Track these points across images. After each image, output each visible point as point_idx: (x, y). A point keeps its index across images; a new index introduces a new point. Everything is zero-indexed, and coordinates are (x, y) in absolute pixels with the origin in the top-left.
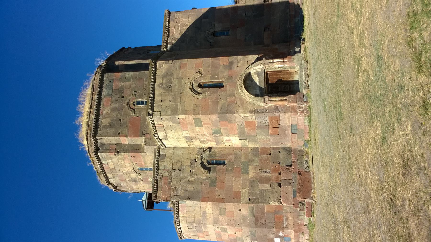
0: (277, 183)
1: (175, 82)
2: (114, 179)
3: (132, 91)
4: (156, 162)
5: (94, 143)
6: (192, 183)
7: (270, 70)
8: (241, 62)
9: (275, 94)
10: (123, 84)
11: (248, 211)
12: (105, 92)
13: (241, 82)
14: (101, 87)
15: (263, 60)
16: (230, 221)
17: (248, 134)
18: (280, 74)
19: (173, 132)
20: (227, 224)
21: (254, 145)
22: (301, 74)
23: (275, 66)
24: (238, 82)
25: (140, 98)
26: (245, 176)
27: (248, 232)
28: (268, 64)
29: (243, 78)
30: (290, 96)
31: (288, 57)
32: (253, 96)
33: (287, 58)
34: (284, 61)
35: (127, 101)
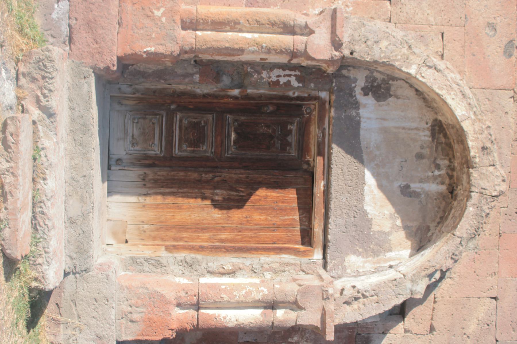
7: (287, 258)
8: (472, 327)
9: (262, 91)
13: (483, 184)
15: (339, 329)
18: (223, 229)
22: (82, 200)
23: (257, 281)
24: (503, 187)
28: (306, 291)
29: (470, 210)
30: (161, 50)
31: (170, 335)
32: (412, 71)
33: (175, 326)
34: (197, 307)
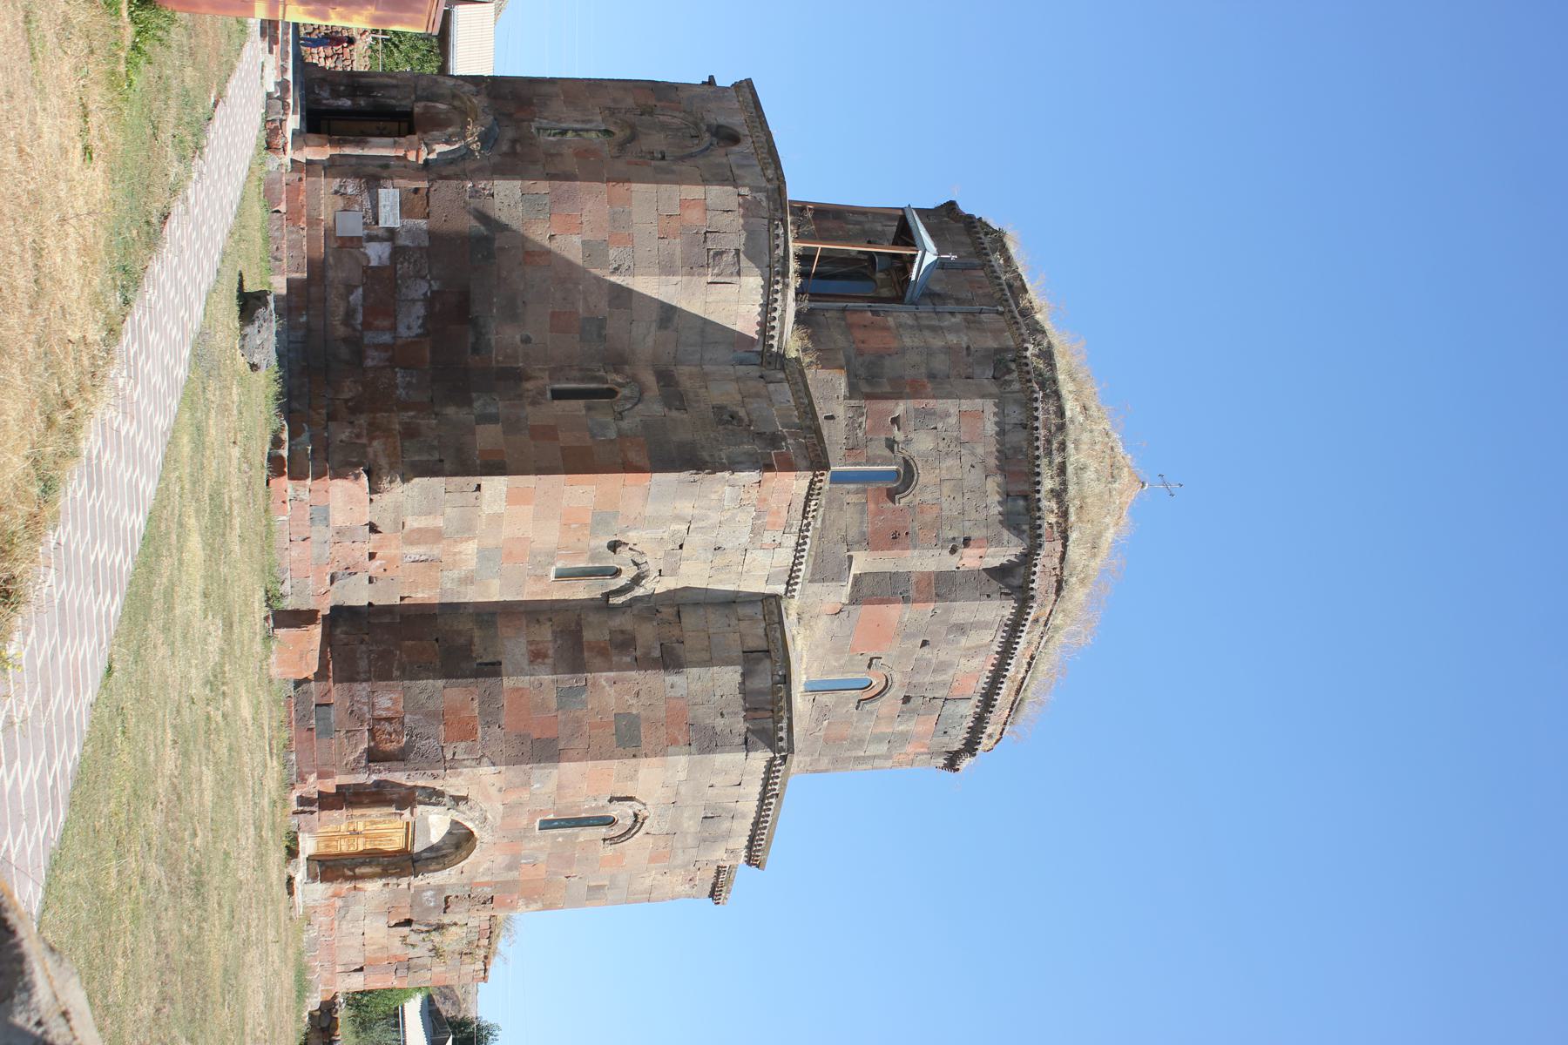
0: (380, 532)
1: (690, 824)
2: (1007, 420)
3: (872, 713)
4: (803, 567)
5: (1033, 581)
6: (678, 518)
8: (481, 870)
10: (901, 728)
11: (493, 339)
12: (968, 709)
14: (980, 722)
16: (564, 299)
17: (472, 693)
19: (718, 694)
20: (581, 287)
21: (455, 628)
25: (848, 699)
26: (490, 542)
27: (502, 249)
35: (893, 691)
